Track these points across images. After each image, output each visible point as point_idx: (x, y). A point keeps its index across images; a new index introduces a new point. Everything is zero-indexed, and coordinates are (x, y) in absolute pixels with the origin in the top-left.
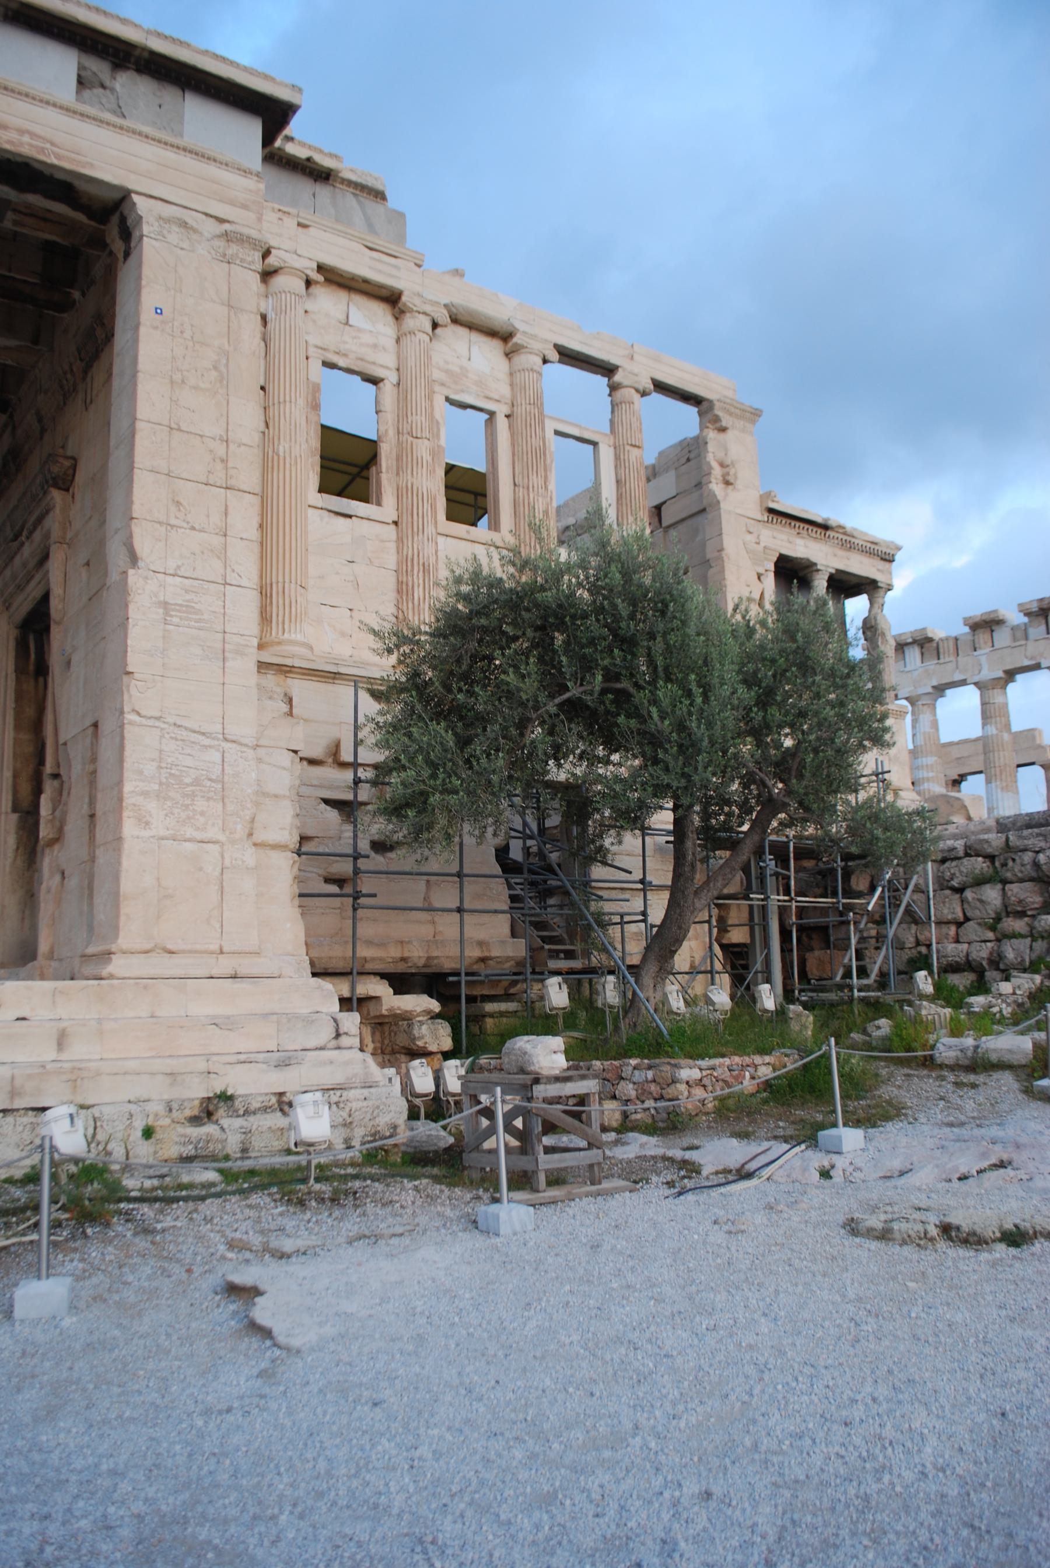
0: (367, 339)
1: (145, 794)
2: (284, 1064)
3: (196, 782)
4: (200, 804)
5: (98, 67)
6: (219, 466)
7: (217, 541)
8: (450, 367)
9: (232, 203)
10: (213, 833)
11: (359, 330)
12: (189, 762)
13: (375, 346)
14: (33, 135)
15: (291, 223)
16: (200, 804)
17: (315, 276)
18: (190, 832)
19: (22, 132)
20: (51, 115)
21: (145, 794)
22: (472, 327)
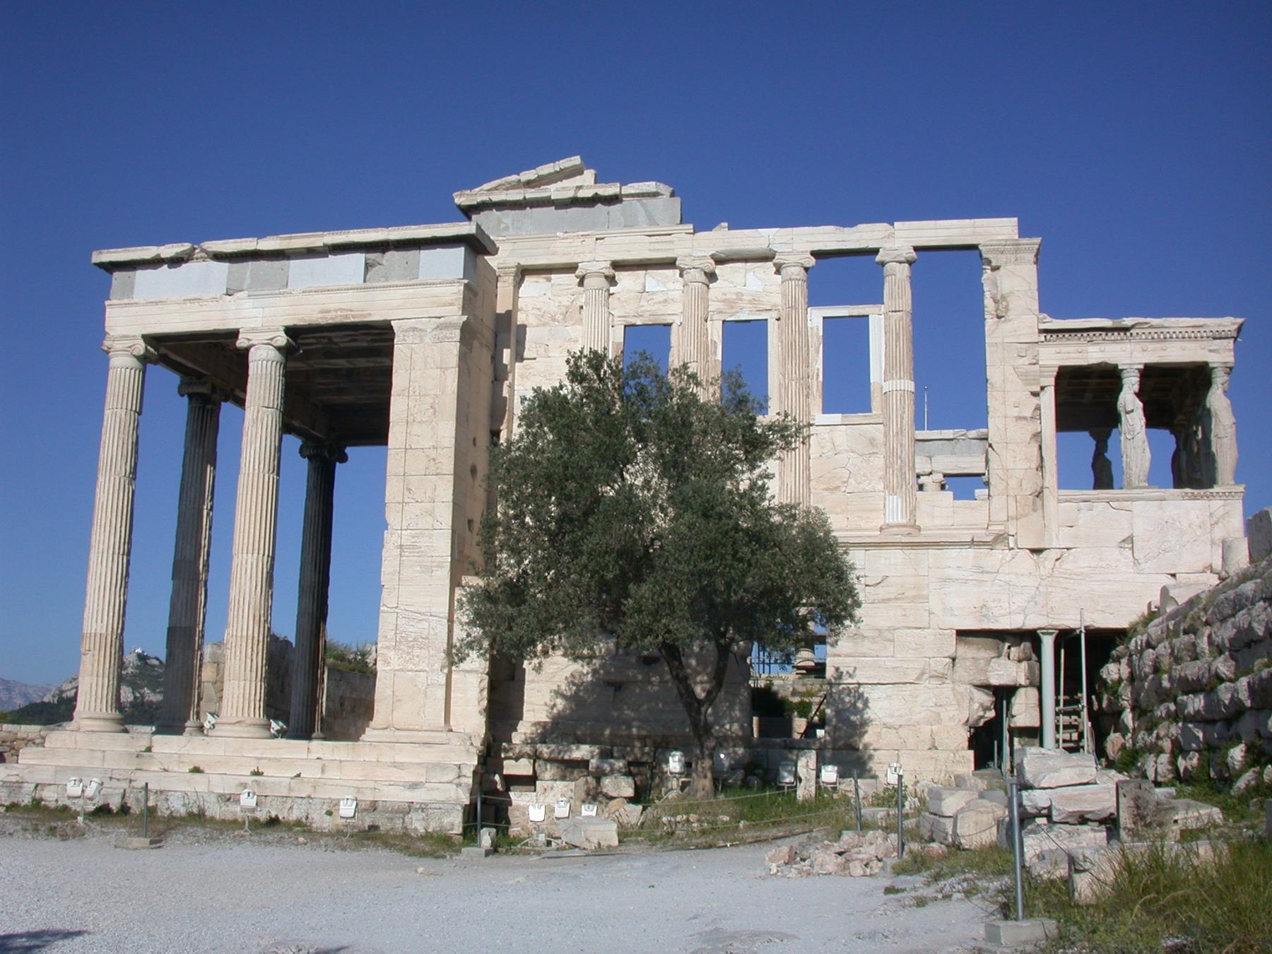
0: (661, 298)
1: (388, 648)
2: (414, 786)
3: (415, 640)
4: (417, 652)
6: (432, 463)
7: (429, 506)
11: (653, 293)
12: (411, 629)
13: (666, 301)
14: (342, 310)
16: (417, 652)
17: (610, 272)
18: (410, 666)
19: (336, 311)
21: (388, 648)
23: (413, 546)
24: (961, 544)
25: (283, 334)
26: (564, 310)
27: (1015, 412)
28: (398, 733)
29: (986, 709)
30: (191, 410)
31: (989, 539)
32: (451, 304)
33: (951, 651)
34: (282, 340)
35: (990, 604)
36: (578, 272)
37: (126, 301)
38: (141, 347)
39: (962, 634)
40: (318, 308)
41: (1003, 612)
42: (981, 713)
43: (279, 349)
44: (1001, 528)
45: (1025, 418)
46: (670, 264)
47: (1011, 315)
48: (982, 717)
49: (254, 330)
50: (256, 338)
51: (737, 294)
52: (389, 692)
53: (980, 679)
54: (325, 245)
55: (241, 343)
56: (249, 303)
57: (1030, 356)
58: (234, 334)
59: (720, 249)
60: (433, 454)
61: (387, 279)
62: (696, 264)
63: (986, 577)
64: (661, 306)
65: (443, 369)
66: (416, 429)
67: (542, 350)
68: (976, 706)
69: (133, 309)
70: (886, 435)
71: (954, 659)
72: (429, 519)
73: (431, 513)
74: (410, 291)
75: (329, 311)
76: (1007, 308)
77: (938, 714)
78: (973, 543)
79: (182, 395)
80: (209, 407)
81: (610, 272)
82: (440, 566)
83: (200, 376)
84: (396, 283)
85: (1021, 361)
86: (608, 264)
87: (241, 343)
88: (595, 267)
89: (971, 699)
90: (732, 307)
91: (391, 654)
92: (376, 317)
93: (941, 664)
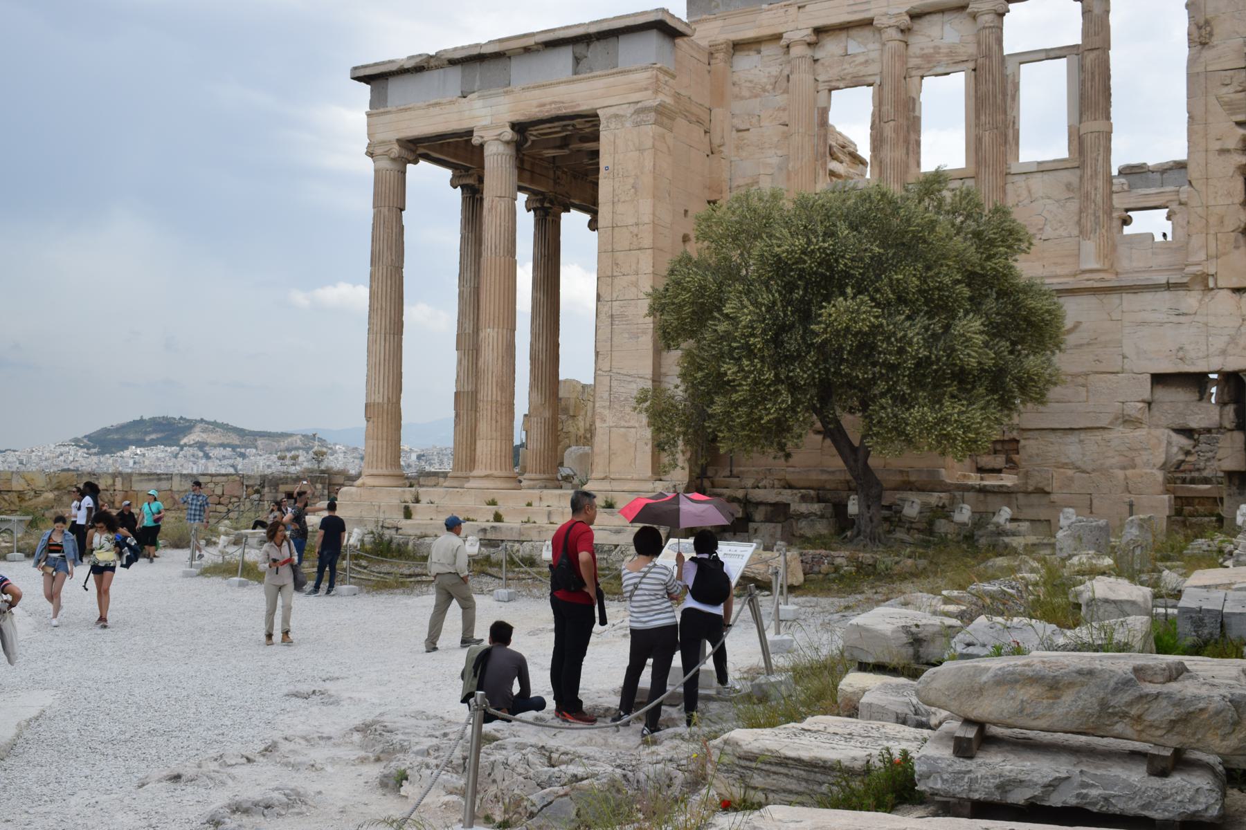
0: (861, 59)
5: (580, 49)
7: (634, 278)
8: (926, 51)
9: (640, 90)
10: (632, 423)
11: (855, 55)
12: (623, 390)
13: (866, 61)
14: (555, 103)
15: (793, 10)
17: (813, 38)
18: (623, 423)
19: (551, 104)
20: (562, 89)
22: (942, 11)
23: (622, 315)
24: (1155, 287)
25: (509, 129)
26: (773, 80)
27: (1218, 145)
28: (614, 483)
29: (1188, 453)
30: (464, 199)
31: (1185, 280)
32: (646, 89)
33: (1147, 395)
34: (509, 134)
35: (1187, 347)
36: (783, 42)
37: (382, 110)
38: (396, 150)
39: (1159, 379)
40: (535, 103)
41: (1201, 354)
42: (1181, 457)
43: (508, 143)
44: (1199, 268)
45: (1228, 151)
46: (868, 23)
47: (1215, 41)
48: (1183, 461)
49: (485, 128)
50: (488, 135)
51: (935, 47)
52: (606, 447)
53: (1179, 422)
54: (537, 44)
55: (476, 140)
56: (478, 104)
57: (1235, 84)
58: (470, 133)
59: (914, 4)
60: (635, 230)
61: (591, 70)
62: (892, 22)
63: (1182, 319)
64: (861, 67)
65: (641, 150)
66: (620, 208)
67: (754, 120)
68: (1175, 450)
69: (387, 118)
70: (1081, 178)
71: (1149, 404)
72: (634, 290)
73: (636, 285)
74: (611, 80)
75: (544, 105)
76: (1211, 34)
77: (1133, 460)
78: (1169, 286)
79: (455, 187)
80: (478, 196)
81: (813, 38)
82: (644, 333)
83: (467, 169)
84: (598, 73)
85: (1225, 90)
86: (809, 31)
87: (476, 140)
88: (797, 36)
89: (1169, 443)
90: (929, 62)
91: (606, 412)
92: (584, 107)
93: (1135, 408)
